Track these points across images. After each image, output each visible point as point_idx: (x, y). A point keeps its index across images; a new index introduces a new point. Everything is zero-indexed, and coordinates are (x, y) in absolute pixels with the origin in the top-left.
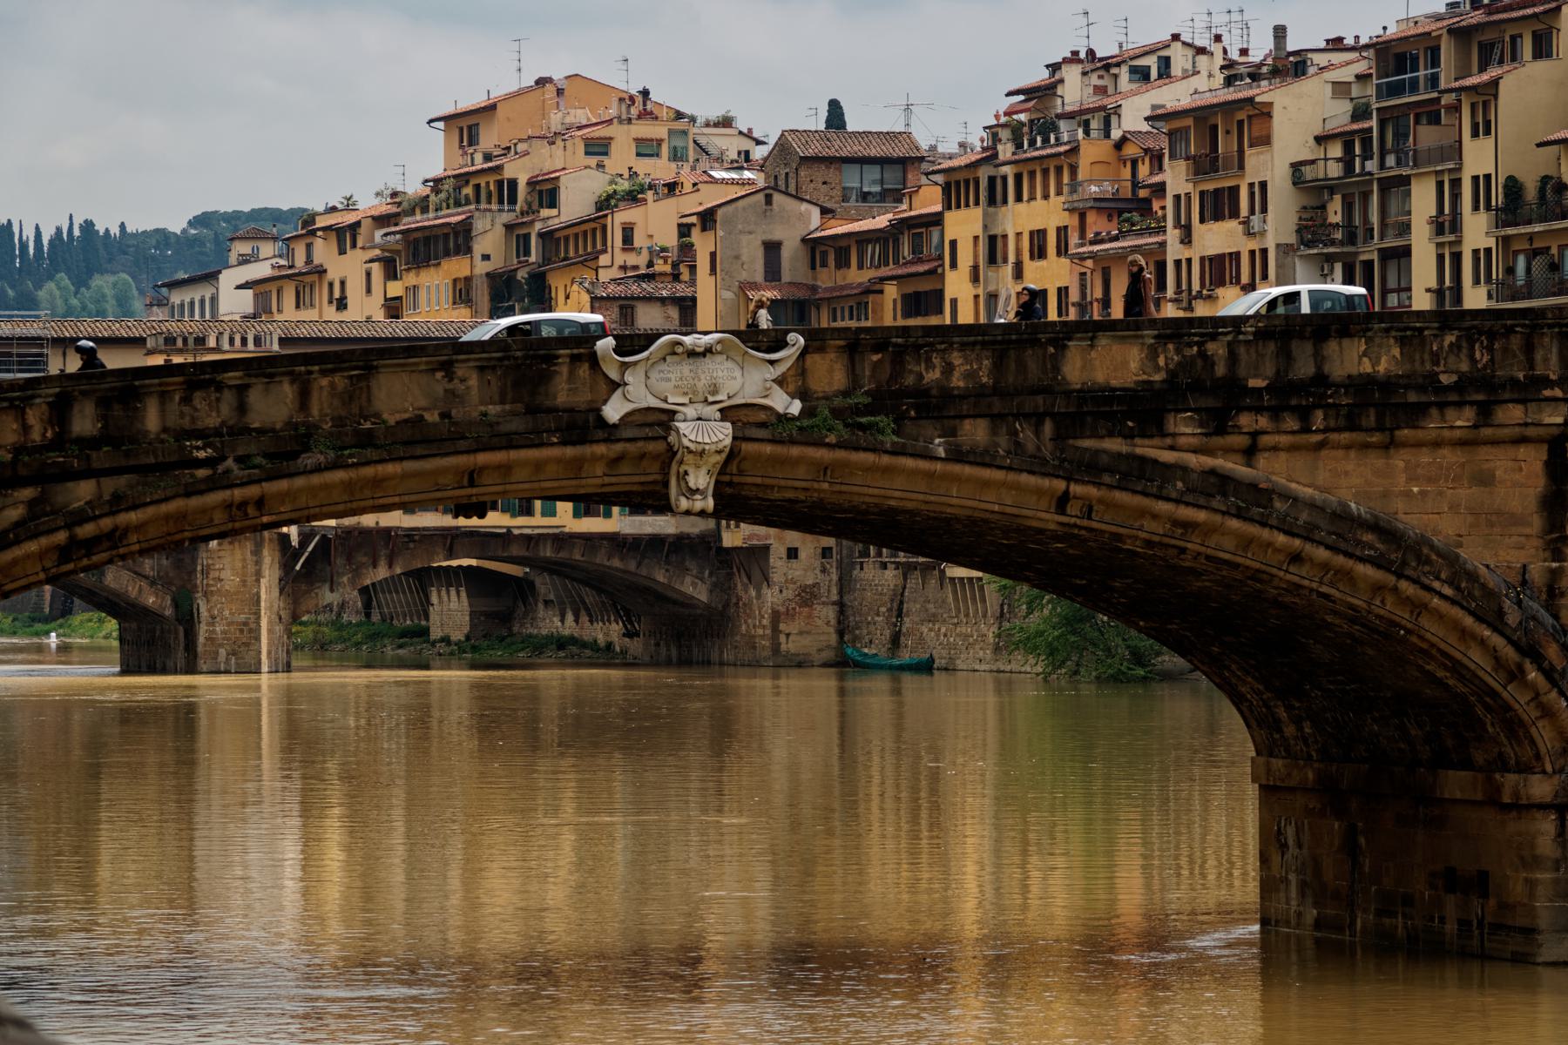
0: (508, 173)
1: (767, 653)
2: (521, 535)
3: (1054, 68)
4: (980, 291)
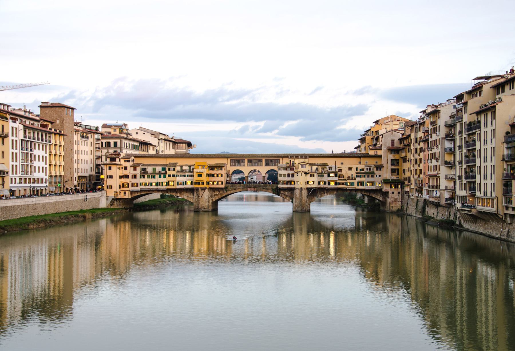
0: (372, 130)
1: (388, 209)
2: (348, 189)
3: (427, 107)
4: (414, 148)
